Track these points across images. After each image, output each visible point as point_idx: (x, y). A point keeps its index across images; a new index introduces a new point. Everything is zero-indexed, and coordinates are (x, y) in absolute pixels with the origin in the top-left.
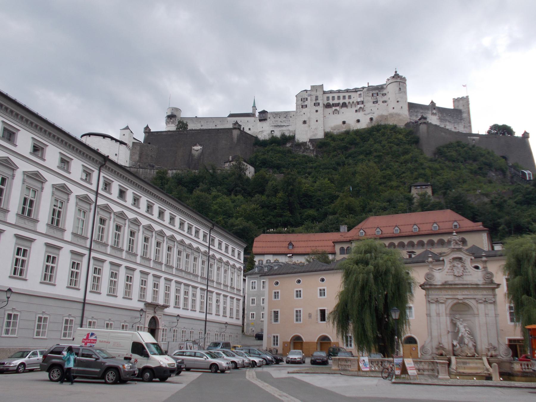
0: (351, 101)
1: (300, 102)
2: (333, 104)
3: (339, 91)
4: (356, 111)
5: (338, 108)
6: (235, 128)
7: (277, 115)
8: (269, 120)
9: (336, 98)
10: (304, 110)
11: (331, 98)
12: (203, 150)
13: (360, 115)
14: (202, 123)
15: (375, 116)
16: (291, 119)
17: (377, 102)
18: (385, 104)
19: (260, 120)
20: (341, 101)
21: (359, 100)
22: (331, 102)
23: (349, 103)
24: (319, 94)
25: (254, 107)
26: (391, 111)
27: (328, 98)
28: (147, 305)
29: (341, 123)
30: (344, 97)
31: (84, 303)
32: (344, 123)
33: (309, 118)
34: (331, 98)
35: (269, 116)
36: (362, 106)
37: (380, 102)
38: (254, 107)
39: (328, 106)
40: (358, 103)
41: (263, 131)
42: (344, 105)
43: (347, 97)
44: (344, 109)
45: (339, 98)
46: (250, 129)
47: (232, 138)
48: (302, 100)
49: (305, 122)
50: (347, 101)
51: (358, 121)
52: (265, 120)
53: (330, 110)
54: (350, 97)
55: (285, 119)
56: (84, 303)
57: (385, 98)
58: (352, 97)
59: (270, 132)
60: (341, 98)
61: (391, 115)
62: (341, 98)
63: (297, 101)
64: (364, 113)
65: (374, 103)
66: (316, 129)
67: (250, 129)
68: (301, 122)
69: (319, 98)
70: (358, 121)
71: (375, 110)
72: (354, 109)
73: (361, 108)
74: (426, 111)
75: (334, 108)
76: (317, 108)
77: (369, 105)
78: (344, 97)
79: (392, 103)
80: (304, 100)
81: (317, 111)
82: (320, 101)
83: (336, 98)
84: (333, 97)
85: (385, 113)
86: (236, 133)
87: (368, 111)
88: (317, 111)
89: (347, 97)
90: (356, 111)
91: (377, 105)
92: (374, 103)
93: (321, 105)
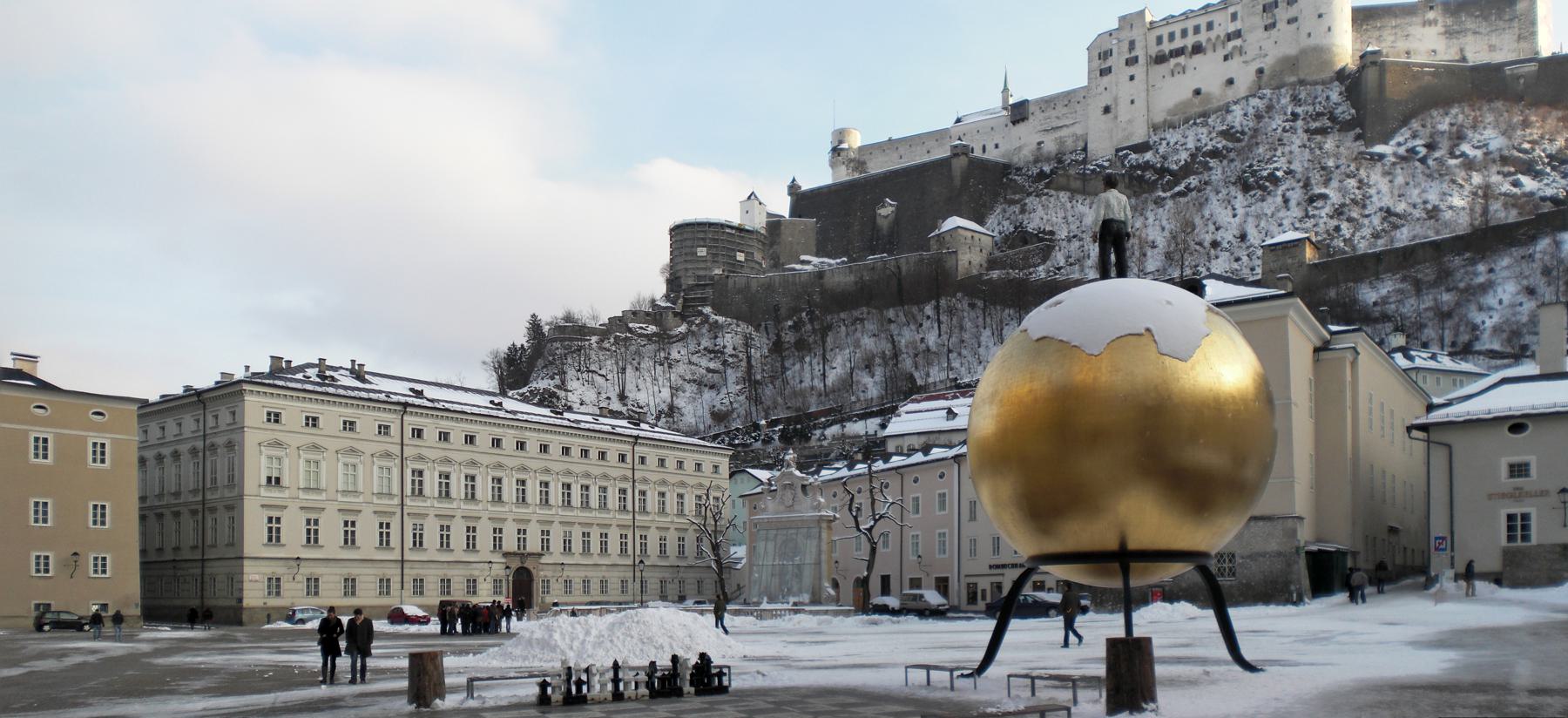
0: (1213, 35)
1: (1097, 63)
2: (1171, 52)
3: (1186, 15)
4: (1226, 58)
5: (1181, 60)
6: (955, 155)
7: (1048, 103)
8: (1031, 118)
9: (1178, 35)
10: (1106, 79)
11: (1165, 39)
12: (898, 208)
13: (1235, 68)
14: (902, 151)
15: (1267, 63)
16: (1078, 107)
17: (1273, 25)
18: (1294, 26)
19: (1014, 123)
20: (1190, 41)
21: (1232, 28)
22: (1167, 47)
23: (1209, 40)
24: (1136, 34)
25: (1006, 90)
26: (1306, 42)
27: (1159, 40)
28: (506, 555)
29: (1189, 94)
30: (1197, 30)
31: (402, 561)
32: (1197, 92)
33: (1116, 99)
34: (1165, 39)
35: (1032, 109)
36: (1237, 42)
37: (1281, 25)
38: (1006, 90)
39: (1160, 59)
40: (1229, 37)
41: (1021, 144)
42: (1198, 49)
43: (1203, 28)
44: (1198, 58)
45: (1184, 33)
46: (997, 146)
47: (951, 178)
48: (1102, 59)
49: (1107, 110)
50: (1202, 37)
51: (1230, 82)
52: (1024, 119)
53: (1163, 69)
54: (1210, 26)
55: (1065, 110)
56: (402, 561)
57: (1292, 11)
58: (1216, 25)
59: (1034, 146)
60: (1191, 32)
61: (1304, 52)
62: (1191, 32)
63: (1090, 61)
64: (1244, 58)
65: (1266, 28)
66: (1130, 121)
67: (997, 146)
68: (1100, 111)
69: (1138, 45)
70: (1230, 82)
71: (1268, 45)
72: (1221, 53)
73: (1235, 48)
74: (1408, 19)
75: (1173, 61)
76: (1132, 70)
77: (1256, 38)
78: (1197, 30)
79: (1307, 24)
80: (1106, 55)
81: (1132, 78)
82: (1139, 51)
83: (1178, 35)
84: (1172, 37)
85: (1292, 51)
86: (959, 164)
87: (1252, 51)
88: (1132, 78)
89: (1203, 28)
90: (1226, 58)
91: (1274, 32)
92: (1266, 28)
93: (1142, 60)
